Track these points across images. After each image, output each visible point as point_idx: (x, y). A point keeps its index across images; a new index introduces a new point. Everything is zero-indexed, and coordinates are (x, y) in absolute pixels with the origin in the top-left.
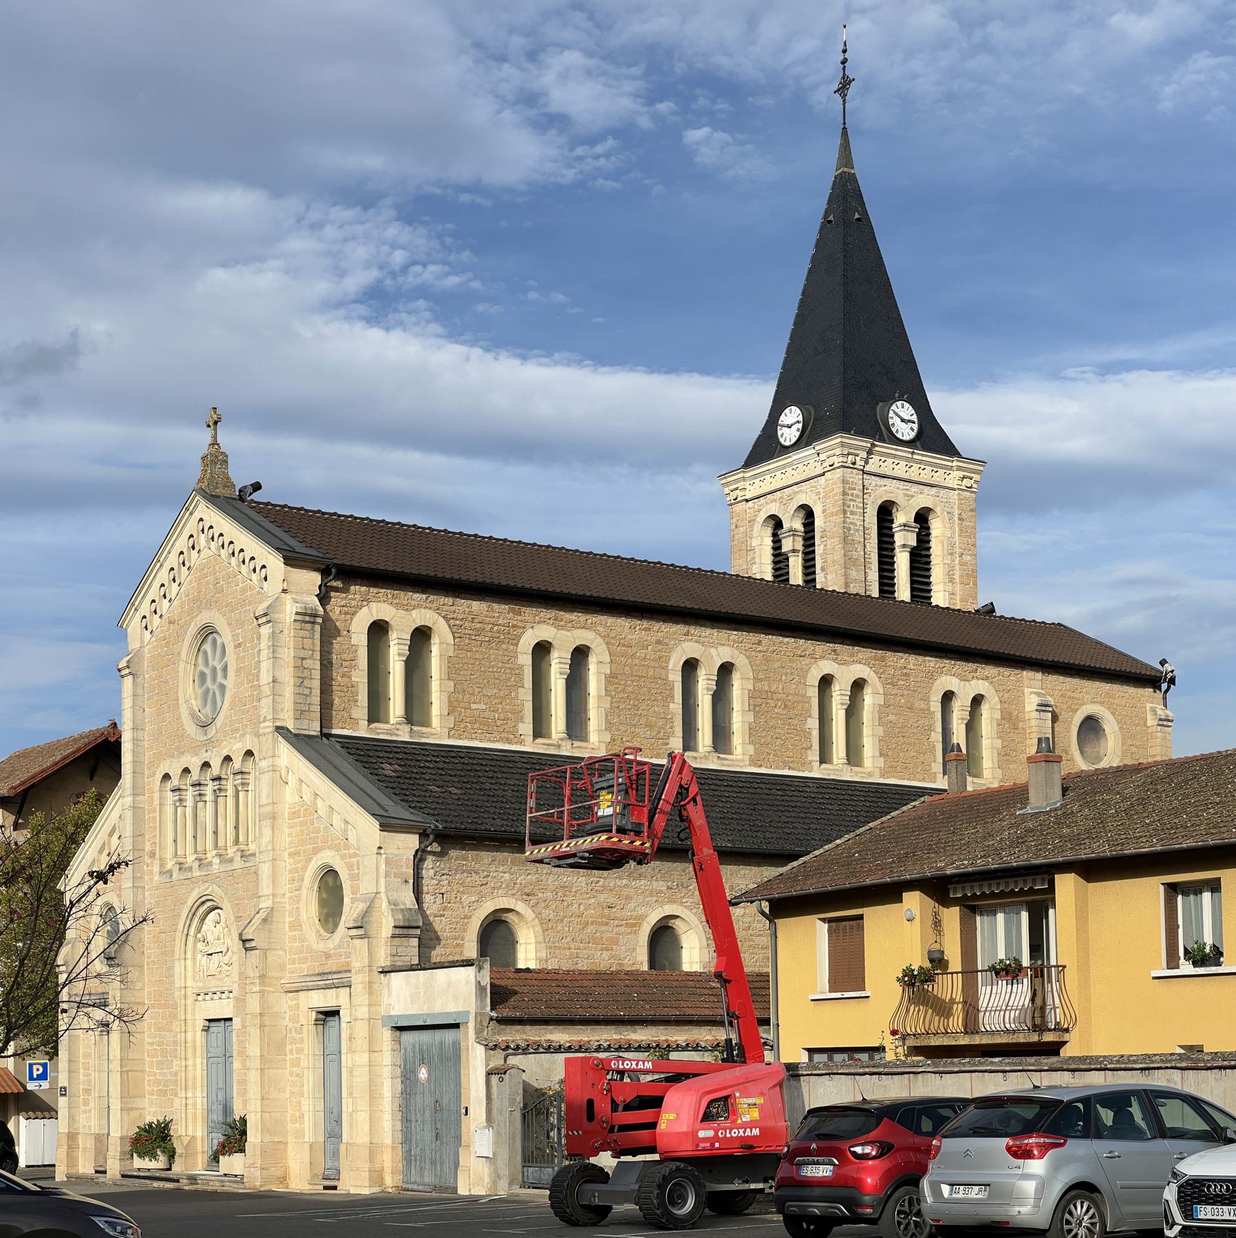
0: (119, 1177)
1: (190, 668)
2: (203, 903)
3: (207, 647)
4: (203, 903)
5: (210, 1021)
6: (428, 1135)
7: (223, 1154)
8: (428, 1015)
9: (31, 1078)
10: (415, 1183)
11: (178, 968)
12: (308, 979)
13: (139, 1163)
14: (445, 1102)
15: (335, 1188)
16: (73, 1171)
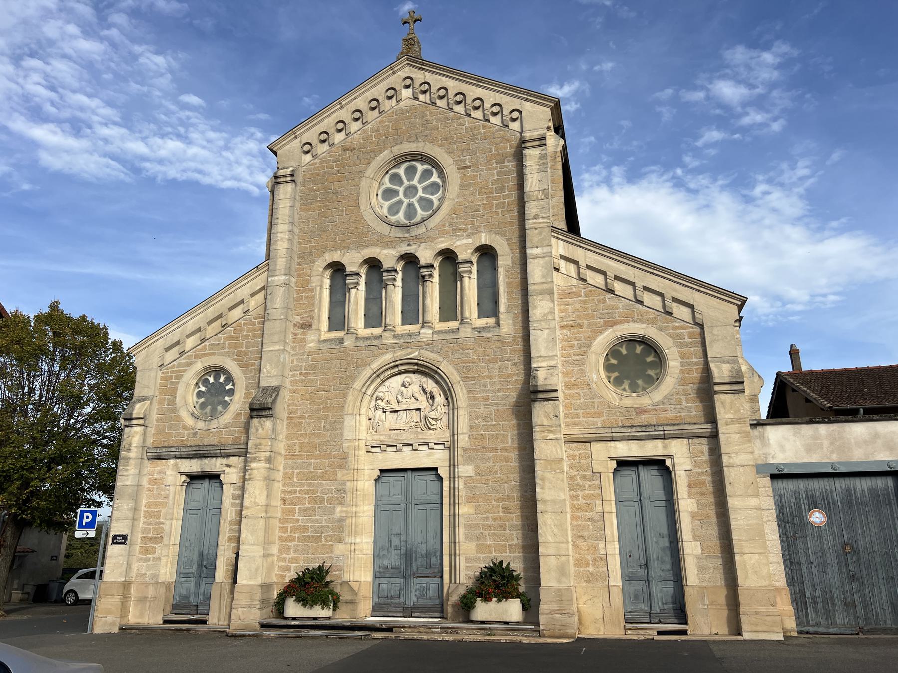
0: (258, 626)
1: (375, 184)
2: (396, 366)
3: (401, 171)
4: (396, 366)
5: (382, 471)
6: (834, 576)
7: (487, 599)
8: (839, 463)
9: (81, 526)
10: (818, 624)
11: (349, 422)
12: (617, 430)
13: (293, 609)
14: (861, 545)
15: (685, 633)
16: (124, 622)
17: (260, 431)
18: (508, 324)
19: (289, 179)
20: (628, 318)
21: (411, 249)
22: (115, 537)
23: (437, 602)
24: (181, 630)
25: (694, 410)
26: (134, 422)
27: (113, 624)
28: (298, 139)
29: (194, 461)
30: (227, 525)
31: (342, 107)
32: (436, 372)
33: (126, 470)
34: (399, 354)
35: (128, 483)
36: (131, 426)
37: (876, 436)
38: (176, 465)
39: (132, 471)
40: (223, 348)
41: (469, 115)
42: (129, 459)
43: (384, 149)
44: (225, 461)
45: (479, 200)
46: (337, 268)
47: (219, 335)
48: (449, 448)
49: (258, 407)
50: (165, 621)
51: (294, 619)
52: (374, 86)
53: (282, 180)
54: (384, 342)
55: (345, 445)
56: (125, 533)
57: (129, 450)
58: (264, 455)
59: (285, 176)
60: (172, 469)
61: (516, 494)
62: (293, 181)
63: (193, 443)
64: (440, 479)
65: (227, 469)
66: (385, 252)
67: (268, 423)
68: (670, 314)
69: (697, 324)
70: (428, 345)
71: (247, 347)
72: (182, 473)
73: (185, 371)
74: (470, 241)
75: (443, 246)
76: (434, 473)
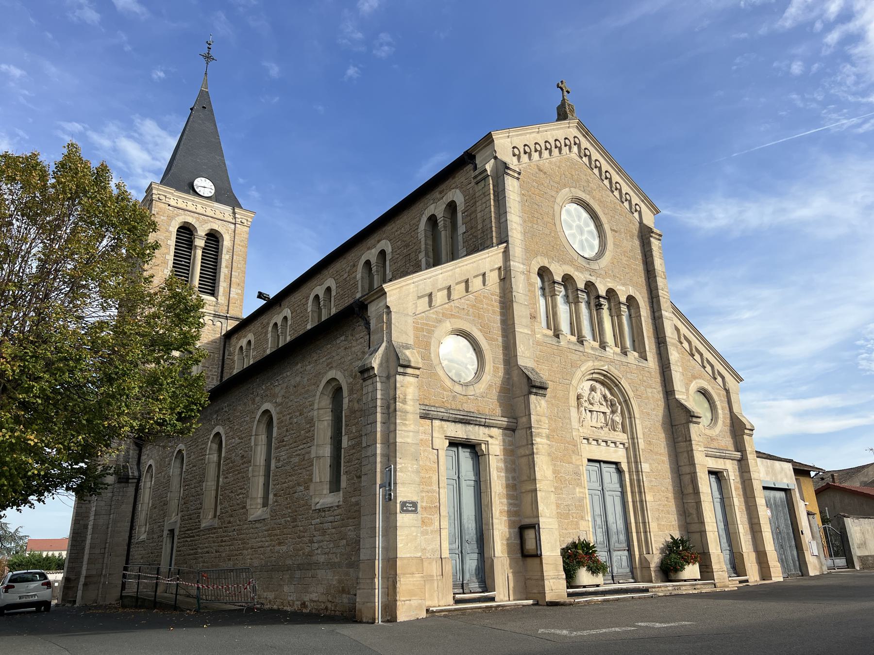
13: (584, 577)
17: (538, 408)
18: (652, 362)
19: (516, 175)
20: (700, 377)
21: (593, 279)
22: (404, 504)
23: (628, 570)
24: (491, 607)
25: (728, 442)
26: (409, 371)
27: (419, 607)
28: (509, 140)
29: (459, 426)
30: (497, 498)
31: (538, 132)
32: (617, 385)
33: (405, 425)
34: (597, 364)
35: (409, 440)
36: (404, 374)
37: (782, 468)
38: (442, 427)
39: (412, 427)
40: (468, 314)
41: (613, 192)
42: (406, 412)
43: (565, 186)
44: (486, 430)
45: (624, 260)
46: (543, 272)
47: (463, 300)
48: (627, 449)
49: (539, 385)
50: (457, 602)
51: (584, 587)
52: (558, 129)
53: (511, 172)
54: (586, 350)
55: (574, 434)
56: (414, 499)
57: (404, 402)
58: (545, 432)
59: (514, 171)
60: (439, 432)
61: (670, 488)
62: (518, 179)
63: (454, 407)
64: (620, 471)
65: (490, 440)
66: (576, 273)
67: (543, 402)
68: (715, 379)
69: (725, 389)
70: (612, 362)
71: (489, 320)
72: (447, 437)
73: (435, 327)
74: (624, 288)
75: (611, 285)
76: (614, 466)
